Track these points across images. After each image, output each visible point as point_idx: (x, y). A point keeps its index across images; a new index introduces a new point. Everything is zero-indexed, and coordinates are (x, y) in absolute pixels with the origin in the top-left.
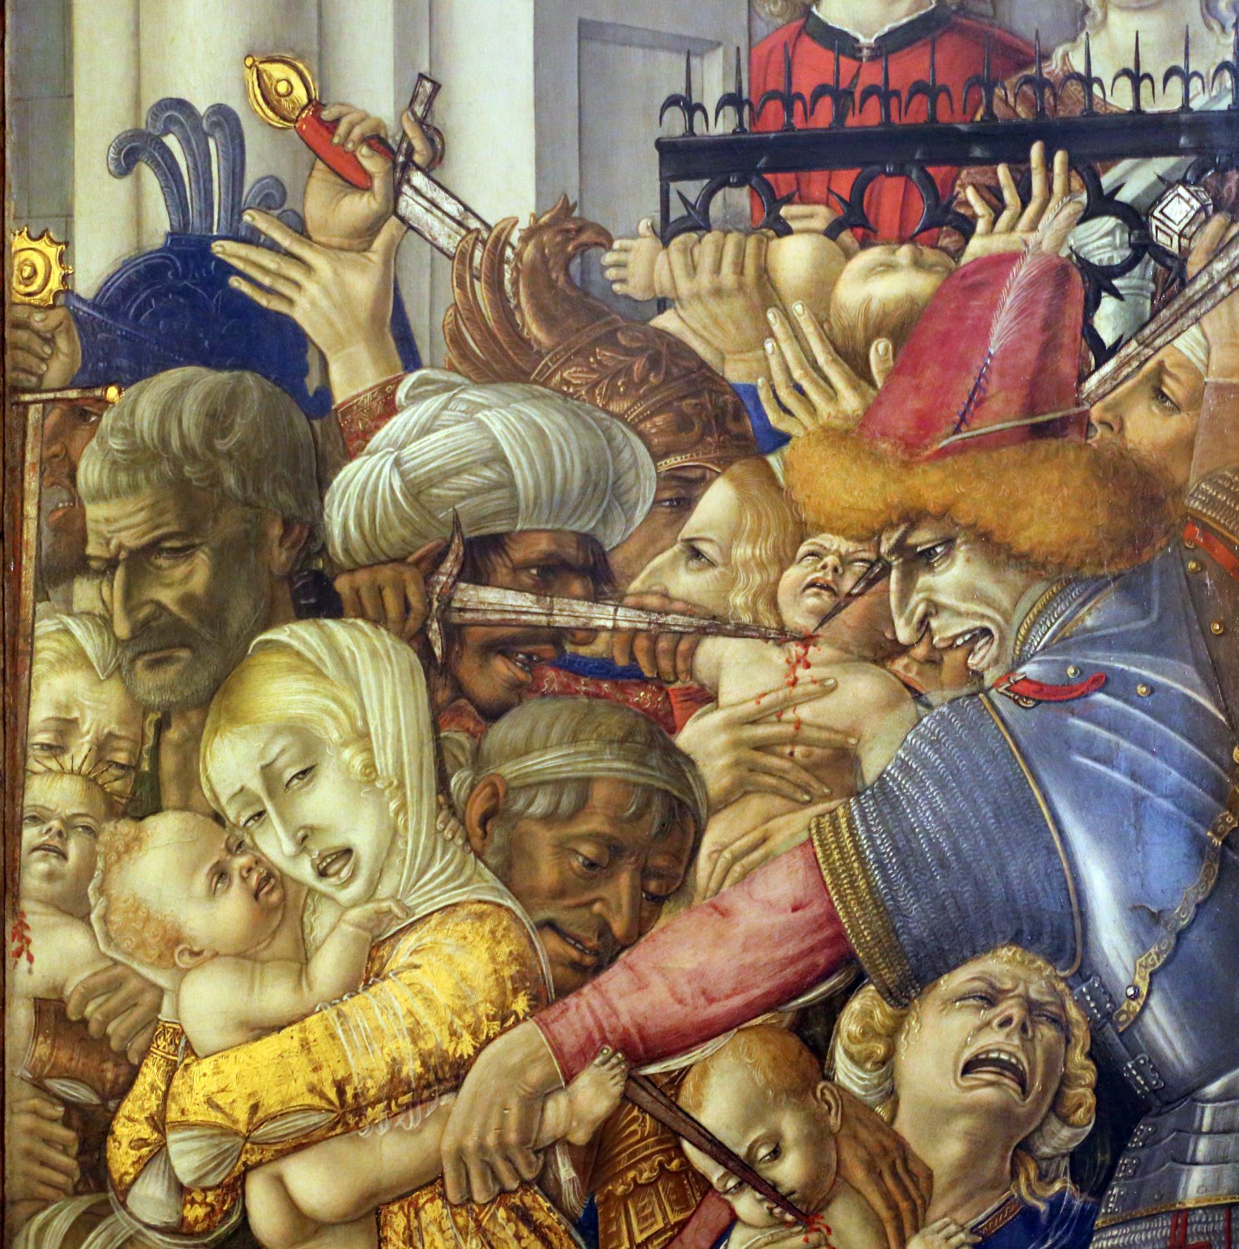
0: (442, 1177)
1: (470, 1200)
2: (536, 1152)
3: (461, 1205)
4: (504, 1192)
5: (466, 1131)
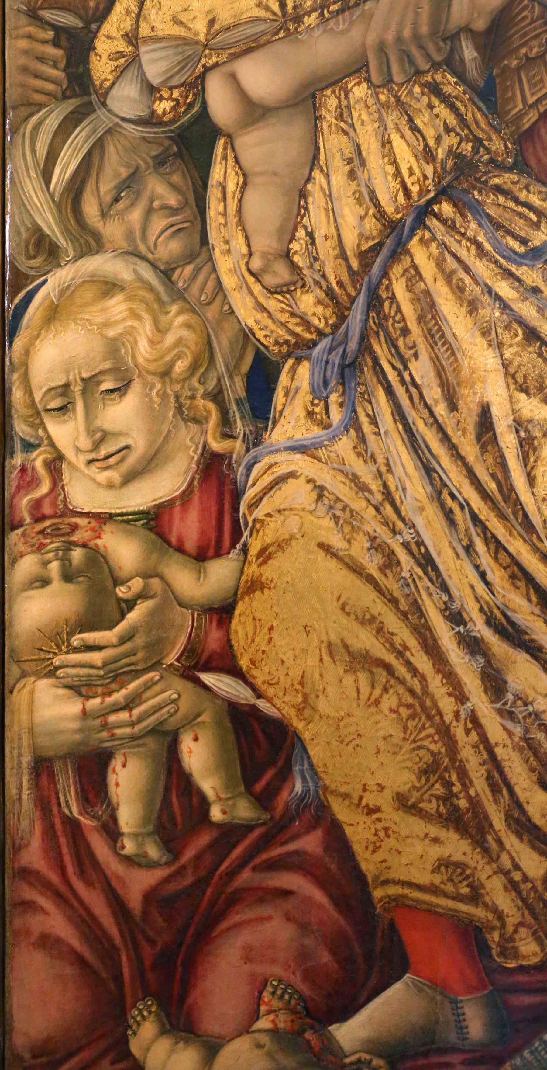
0: (367, 66)
1: (391, 81)
2: (444, 40)
3: (383, 86)
4: (419, 73)
5: (386, 28)
